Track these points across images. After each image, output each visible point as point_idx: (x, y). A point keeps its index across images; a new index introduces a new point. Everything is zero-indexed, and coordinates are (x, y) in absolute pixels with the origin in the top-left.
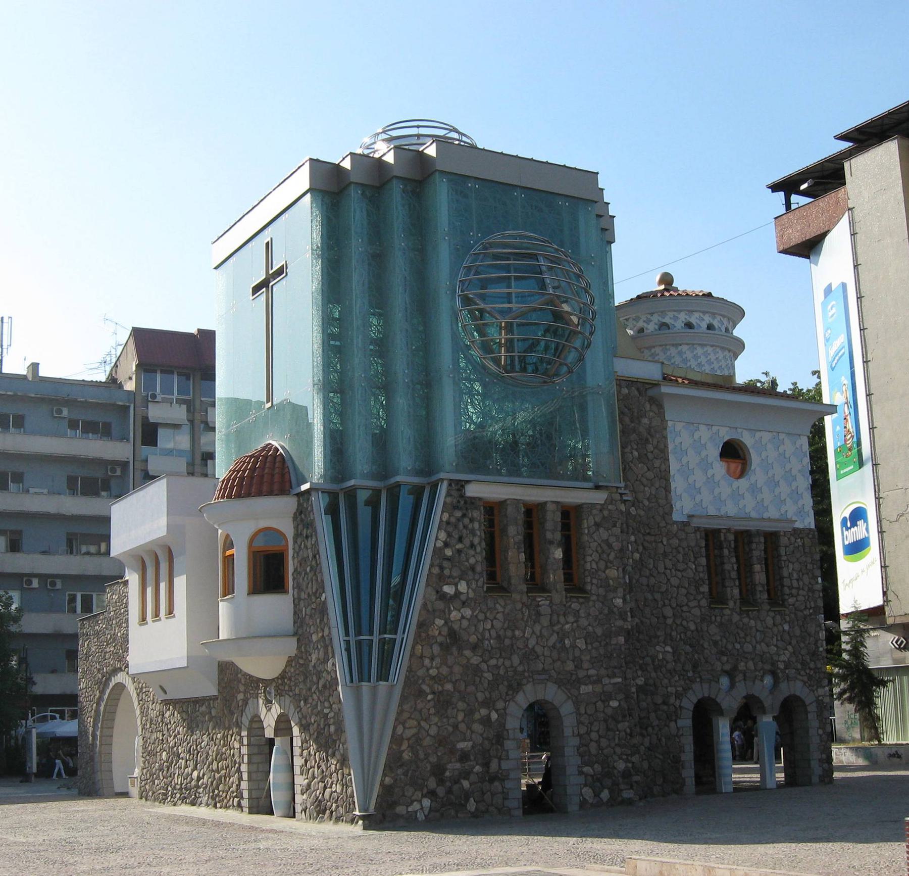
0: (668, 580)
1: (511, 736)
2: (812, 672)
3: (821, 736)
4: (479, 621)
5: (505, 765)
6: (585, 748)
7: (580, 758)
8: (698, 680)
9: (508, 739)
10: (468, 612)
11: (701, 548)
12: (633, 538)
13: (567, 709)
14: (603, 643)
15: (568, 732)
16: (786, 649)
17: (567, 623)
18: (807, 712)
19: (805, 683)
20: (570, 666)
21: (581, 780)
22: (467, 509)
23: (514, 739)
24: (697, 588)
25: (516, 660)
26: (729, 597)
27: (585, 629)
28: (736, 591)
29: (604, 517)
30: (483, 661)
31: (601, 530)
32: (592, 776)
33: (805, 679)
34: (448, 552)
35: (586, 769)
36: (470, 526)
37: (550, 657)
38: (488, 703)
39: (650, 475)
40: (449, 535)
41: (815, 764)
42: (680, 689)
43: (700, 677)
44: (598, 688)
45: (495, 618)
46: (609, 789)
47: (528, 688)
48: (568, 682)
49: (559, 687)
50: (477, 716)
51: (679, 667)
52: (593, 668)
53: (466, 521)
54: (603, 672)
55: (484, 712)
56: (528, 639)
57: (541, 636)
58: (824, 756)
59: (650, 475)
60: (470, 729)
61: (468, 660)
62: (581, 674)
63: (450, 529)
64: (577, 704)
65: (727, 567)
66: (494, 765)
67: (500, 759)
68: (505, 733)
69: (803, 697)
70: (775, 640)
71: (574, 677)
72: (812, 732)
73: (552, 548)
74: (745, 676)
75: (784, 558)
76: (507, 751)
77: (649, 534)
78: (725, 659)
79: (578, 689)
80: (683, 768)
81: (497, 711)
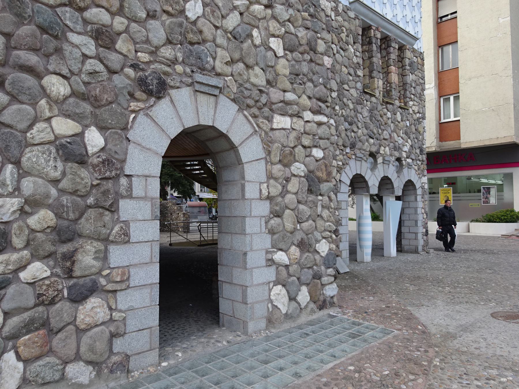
0: (334, 54)
1: (138, 190)
2: (420, 163)
3: (423, 214)
5: (118, 256)
6: (277, 220)
7: (269, 237)
8: (354, 157)
9: (130, 196)
11: (359, 35)
13: (250, 150)
14: (307, 57)
15: (251, 191)
16: (407, 142)
18: (416, 195)
19: (416, 171)
20: (258, 77)
21: (270, 274)
23: (144, 198)
24: (355, 73)
25: (157, 31)
26: (376, 86)
28: (381, 83)
32: (287, 267)
33: (416, 168)
35: (281, 257)
41: (420, 236)
42: (341, 163)
43: (355, 155)
44: (299, 124)
46: (307, 285)
47: (182, 95)
48: (254, 104)
49: (240, 110)
50: (39, 132)
51: (340, 143)
52: (294, 91)
54: (305, 100)
55: (64, 127)
58: (424, 230)
62: (275, 95)
64: (267, 144)
65: (375, 60)
66: (87, 260)
67: (106, 240)
68: (123, 181)
69: (415, 183)
70: (401, 132)
71: (264, 99)
72: (420, 211)
74: (384, 159)
75: (408, 67)
78: (372, 141)
79: (270, 119)
80: (340, 241)
81: (102, 129)
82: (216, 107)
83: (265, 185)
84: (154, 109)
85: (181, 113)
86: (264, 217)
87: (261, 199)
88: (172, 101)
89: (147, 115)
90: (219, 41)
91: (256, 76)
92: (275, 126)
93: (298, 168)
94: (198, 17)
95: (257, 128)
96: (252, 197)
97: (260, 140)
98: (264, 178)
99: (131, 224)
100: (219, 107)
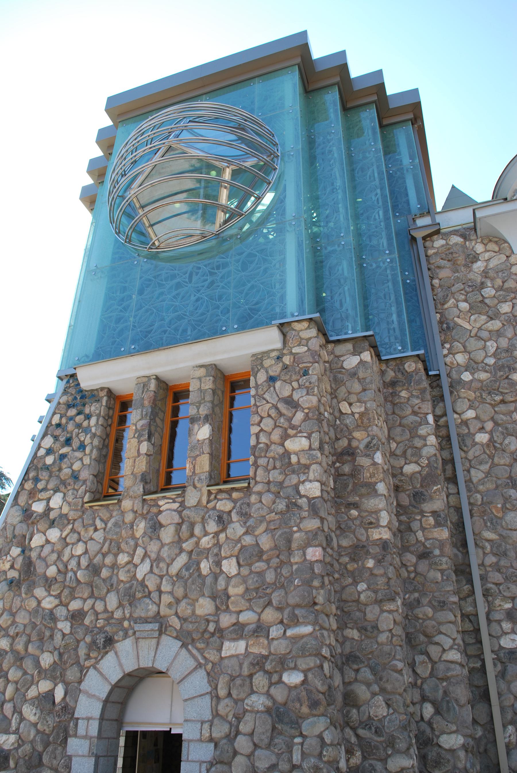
1: (81, 731)
4: (67, 545)
9: (75, 736)
10: (54, 534)
12: (471, 414)
14: (275, 561)
17: (206, 534)
20: (205, 606)
22: (84, 405)
23: (85, 737)
27: (239, 540)
29: (285, 367)
30: (61, 604)
31: (278, 384)
34: (49, 460)
36: (85, 424)
37: (171, 593)
38: (55, 673)
39: (496, 325)
40: (56, 438)
45: (91, 539)
47: (125, 646)
49: (184, 645)
50: (32, 693)
53: (79, 419)
55: (44, 686)
56: (136, 566)
57: (159, 559)
59: (496, 325)
60: (21, 713)
61: (39, 602)
62: (226, 620)
63: (58, 432)
71: (211, 627)
73: (196, 427)
76: (70, 758)
77: (503, 402)
82: (157, 648)
83: (206, 726)
84: (101, 662)
85: (123, 661)
86: (206, 762)
87: (201, 740)
88: (116, 653)
89: (95, 668)
90: (163, 589)
91: (202, 606)
92: (223, 655)
93: (258, 702)
94: (145, 575)
95: (202, 661)
96: (191, 738)
97: (205, 673)
98: (208, 716)
99: (73, 758)
100: (160, 647)
